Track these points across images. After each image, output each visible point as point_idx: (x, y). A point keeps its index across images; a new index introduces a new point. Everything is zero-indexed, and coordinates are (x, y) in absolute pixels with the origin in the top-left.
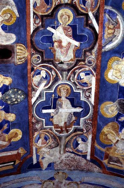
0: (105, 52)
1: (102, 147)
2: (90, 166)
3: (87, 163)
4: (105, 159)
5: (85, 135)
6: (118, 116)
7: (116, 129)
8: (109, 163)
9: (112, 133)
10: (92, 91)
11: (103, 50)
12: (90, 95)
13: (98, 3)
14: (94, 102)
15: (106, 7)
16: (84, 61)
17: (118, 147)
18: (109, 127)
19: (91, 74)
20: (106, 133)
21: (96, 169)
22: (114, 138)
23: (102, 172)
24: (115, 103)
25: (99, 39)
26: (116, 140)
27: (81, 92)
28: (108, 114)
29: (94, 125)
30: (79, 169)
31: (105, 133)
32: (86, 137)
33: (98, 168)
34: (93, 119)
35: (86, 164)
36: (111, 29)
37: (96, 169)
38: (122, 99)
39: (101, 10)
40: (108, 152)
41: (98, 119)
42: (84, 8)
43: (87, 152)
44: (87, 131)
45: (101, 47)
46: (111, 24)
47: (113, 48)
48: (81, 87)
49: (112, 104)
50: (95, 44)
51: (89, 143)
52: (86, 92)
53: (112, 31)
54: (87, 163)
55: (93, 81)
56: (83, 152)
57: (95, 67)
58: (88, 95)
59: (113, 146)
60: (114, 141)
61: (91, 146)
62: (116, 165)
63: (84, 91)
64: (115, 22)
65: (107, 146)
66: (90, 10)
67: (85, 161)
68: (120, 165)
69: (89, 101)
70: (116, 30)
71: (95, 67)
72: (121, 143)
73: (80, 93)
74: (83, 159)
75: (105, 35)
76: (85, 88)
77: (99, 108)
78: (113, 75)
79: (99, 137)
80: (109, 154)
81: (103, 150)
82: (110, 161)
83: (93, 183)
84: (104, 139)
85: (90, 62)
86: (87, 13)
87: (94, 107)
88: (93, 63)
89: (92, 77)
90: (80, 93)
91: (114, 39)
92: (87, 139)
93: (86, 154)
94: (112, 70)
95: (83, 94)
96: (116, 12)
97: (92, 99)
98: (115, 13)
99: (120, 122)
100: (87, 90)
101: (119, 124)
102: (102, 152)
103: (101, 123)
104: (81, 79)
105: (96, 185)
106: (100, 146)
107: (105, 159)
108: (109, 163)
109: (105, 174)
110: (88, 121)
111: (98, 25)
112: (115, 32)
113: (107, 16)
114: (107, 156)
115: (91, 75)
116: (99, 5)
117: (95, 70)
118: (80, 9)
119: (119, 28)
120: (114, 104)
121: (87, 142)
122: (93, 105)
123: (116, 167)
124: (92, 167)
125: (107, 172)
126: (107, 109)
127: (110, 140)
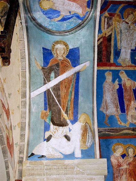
1: (120, 10)
40: (116, 16)
60: (127, 21)
81: (118, 12)
102: (116, 10)
106: (121, 9)
107: (108, 13)
108: (105, 18)
114: (111, 15)
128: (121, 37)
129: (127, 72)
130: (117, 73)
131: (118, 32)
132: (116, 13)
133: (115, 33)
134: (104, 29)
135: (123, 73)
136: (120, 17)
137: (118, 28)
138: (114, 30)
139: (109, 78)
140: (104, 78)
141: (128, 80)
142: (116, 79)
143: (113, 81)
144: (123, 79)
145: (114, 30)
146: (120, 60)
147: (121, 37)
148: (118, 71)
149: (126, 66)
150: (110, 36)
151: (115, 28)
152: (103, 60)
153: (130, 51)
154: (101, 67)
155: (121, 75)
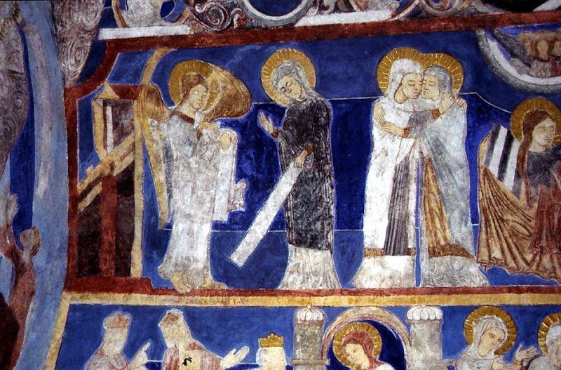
0: (475, 42)
1: (155, 74)
2: (78, 43)
3: (86, 32)
4: (118, 90)
5: (187, 12)
6: (275, 111)
7: (229, 110)
8: (106, 103)
9: (211, 99)
11: (482, 33)
12: (326, 8)
14: (305, 27)
17: (169, 125)
18: (229, 87)
19: (398, 5)
20: (209, 80)
21: (72, 65)
22: (197, 106)
23: (68, 84)
24: (315, 94)
25: (516, 14)
26: (191, 115)
28: (273, 76)
29: (227, 38)
30: (58, 7)
31: (207, 75)
32: (181, 16)
33: (80, 72)
34: (248, 29)
35: (83, 29)
37: (73, 65)
38: (331, 113)
40: (142, 95)
41: (248, 48)
43: (125, 26)
44: (201, 17)
45: (490, 24)
47: (490, 63)
49: (307, 84)
51: (160, 28)
53: (543, 53)
54: (86, 32)
56: (124, 14)
57: (423, 14)
59: (167, 110)
60: (186, 110)
61: (153, 37)
62: (106, 126)
65: (165, 88)
67: (91, 22)
68: (110, 140)
69: (307, 9)
70: (548, 65)
71: (423, 14)
72: (185, 133)
74: (99, 16)
75: (529, 34)
77: (287, 44)
78: (404, 74)
79: (188, 57)
80: (135, 98)
81: (147, 79)
82: (113, 107)
83: (32, 66)
84: (184, 76)
87: (289, 27)
88: (435, 5)
89: (391, 8)
91: (518, 62)
92: (174, 20)
93: (118, 23)
94: (418, 69)
97: (313, 19)
99: (253, 117)
101: (248, 117)
102: (137, 74)
103: (237, 58)
105: (30, 81)
107: (115, 88)
109: (65, 96)
110: (237, 16)
112: (542, 64)
114: (127, 94)
117: (416, 14)
120: (311, 90)
121: (163, 22)
123: (98, 128)
124: (74, 49)
125: (75, 102)
126: (288, 72)
127: (186, 96)
128: (169, 174)
129: (195, 319)
130: (151, 318)
131: (157, 157)
132: (141, 86)
133: (146, 161)
134: (105, 147)
135: (177, 318)
136: (158, 99)
137: (153, 141)
138: (139, 151)
139: (115, 337)
140: (96, 339)
141: (192, 347)
142: (143, 342)
143: (130, 350)
144: (169, 344)
145: (139, 151)
146: (167, 268)
147: (169, 174)
148: (159, 312)
149: (193, 293)
150: (129, 171)
151: (143, 140)
152: (104, 267)
153: (207, 230)
154: (91, 295)
155: (164, 328)
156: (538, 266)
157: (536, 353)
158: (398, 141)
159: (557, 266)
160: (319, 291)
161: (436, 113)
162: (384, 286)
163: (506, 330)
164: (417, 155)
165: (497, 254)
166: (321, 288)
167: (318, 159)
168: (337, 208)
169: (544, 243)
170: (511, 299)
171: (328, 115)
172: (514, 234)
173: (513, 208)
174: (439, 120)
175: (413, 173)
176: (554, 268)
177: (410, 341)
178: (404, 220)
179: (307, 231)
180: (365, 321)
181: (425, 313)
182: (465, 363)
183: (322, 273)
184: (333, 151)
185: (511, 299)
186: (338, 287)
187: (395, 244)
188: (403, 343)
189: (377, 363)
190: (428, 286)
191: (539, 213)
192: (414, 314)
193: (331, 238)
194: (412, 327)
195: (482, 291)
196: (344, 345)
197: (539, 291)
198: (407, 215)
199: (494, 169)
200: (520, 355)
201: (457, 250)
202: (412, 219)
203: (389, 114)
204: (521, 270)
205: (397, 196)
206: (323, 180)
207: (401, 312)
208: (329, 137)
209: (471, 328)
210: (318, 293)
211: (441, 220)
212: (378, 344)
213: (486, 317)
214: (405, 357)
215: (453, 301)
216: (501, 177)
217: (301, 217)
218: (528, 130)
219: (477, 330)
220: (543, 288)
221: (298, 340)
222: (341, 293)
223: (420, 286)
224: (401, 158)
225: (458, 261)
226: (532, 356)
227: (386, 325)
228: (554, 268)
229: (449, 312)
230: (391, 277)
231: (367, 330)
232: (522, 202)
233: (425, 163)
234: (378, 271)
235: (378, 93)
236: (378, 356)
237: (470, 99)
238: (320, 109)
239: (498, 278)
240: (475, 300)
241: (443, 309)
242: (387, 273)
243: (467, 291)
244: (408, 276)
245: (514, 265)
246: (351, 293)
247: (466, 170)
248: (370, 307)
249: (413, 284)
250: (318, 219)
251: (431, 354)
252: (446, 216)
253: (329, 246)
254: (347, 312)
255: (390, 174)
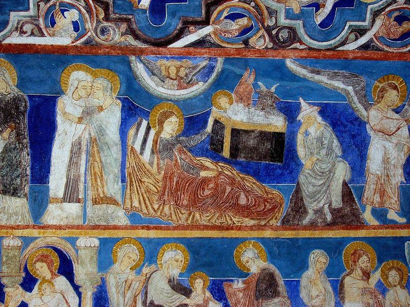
0: (128, 64)
10: (37, 38)
11: (133, 58)
12: (26, 33)
13: (228, 43)
15: (220, 60)
16: (107, 18)
19: (76, 35)
24: (16, 90)
25: (156, 48)
27: (32, 12)
36: (178, 71)
38: (28, 104)
39: (215, 51)
42: (221, 17)
45: (138, 53)
46: (187, 71)
47: (138, 78)
48: (42, 13)
49: (11, 83)
50: (145, 41)
52: (32, 23)
53: (173, 75)
55: (63, 38)
57: (94, 42)
58: (25, 29)
63: (34, 19)
64: (191, 80)
66: (216, 30)
69: (11, 32)
70: (175, 82)
71: (94, 42)
73: (28, 9)
75: (164, 61)
76: (41, 21)
78: (80, 81)
85: (104, 31)
86: (211, 23)
88: (102, 37)
89: (71, 37)
90: (28, 9)
91: (156, 78)
94: (89, 78)
95: (25, 17)
96: (211, 80)
97: (16, 39)
98: (209, 79)
100: (38, 26)
104: (63, 11)
111: (185, 47)
112: (172, 81)
113: (204, 63)
115: (75, 34)
116: (226, 45)
117: (87, 43)
118: (220, 8)
119: (180, 87)
120: (14, 87)
122: (3, 43)
156: (161, 212)
157: (155, 269)
158: (74, 125)
159: (173, 213)
160: (18, 226)
161: (101, 109)
162: (62, 223)
163: (138, 254)
164: (87, 136)
165: (136, 204)
166: (20, 224)
167: (18, 135)
168: (32, 169)
169: (166, 198)
170: (143, 234)
171: (26, 105)
172: (148, 191)
173: (148, 173)
174: (102, 113)
175: (84, 148)
176: (171, 213)
177: (78, 261)
178: (77, 180)
179: (10, 185)
180: (48, 247)
181: (88, 242)
182: (111, 275)
183: (20, 213)
184: (30, 130)
185: (143, 234)
186: (32, 223)
187: (71, 195)
188: (73, 262)
189: (56, 275)
190: (91, 224)
191: (165, 177)
192: (81, 242)
193: (27, 189)
194: (79, 252)
195: (126, 228)
196: (35, 263)
197: (161, 228)
198: (79, 176)
199: (137, 147)
200: (145, 270)
201: (112, 201)
202: (82, 179)
203: (67, 108)
204: (150, 215)
205: (73, 162)
206: (22, 150)
207: (73, 241)
208: (26, 120)
209: (116, 252)
210: (18, 227)
211: (102, 180)
212: (57, 263)
213: (126, 245)
214: (74, 271)
215: (106, 234)
216: (142, 153)
217: (6, 175)
218: (161, 123)
219: (120, 254)
220: (163, 227)
221: (4, 260)
222: (34, 227)
223: (86, 224)
224: (76, 138)
225: (111, 208)
226: (152, 271)
227: (62, 249)
228: (171, 213)
229: (104, 242)
230: (67, 218)
231: (50, 253)
232: (154, 170)
233: (93, 141)
234: (55, 214)
235: (61, 93)
236: (57, 271)
237: (124, 101)
238: (20, 100)
239: (136, 221)
240: (120, 234)
241: (99, 239)
242: (64, 215)
243: (115, 228)
244: (78, 217)
245: (146, 212)
246: (40, 228)
247: (120, 147)
248: (52, 238)
249: (81, 223)
250: (18, 177)
251: (91, 270)
252: (105, 177)
253: (25, 195)
254: (38, 240)
255: (68, 148)
